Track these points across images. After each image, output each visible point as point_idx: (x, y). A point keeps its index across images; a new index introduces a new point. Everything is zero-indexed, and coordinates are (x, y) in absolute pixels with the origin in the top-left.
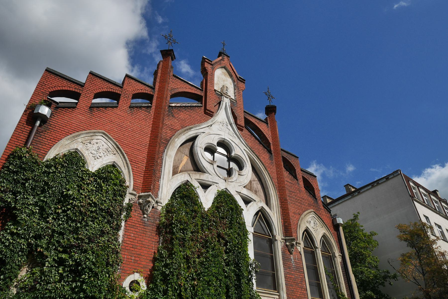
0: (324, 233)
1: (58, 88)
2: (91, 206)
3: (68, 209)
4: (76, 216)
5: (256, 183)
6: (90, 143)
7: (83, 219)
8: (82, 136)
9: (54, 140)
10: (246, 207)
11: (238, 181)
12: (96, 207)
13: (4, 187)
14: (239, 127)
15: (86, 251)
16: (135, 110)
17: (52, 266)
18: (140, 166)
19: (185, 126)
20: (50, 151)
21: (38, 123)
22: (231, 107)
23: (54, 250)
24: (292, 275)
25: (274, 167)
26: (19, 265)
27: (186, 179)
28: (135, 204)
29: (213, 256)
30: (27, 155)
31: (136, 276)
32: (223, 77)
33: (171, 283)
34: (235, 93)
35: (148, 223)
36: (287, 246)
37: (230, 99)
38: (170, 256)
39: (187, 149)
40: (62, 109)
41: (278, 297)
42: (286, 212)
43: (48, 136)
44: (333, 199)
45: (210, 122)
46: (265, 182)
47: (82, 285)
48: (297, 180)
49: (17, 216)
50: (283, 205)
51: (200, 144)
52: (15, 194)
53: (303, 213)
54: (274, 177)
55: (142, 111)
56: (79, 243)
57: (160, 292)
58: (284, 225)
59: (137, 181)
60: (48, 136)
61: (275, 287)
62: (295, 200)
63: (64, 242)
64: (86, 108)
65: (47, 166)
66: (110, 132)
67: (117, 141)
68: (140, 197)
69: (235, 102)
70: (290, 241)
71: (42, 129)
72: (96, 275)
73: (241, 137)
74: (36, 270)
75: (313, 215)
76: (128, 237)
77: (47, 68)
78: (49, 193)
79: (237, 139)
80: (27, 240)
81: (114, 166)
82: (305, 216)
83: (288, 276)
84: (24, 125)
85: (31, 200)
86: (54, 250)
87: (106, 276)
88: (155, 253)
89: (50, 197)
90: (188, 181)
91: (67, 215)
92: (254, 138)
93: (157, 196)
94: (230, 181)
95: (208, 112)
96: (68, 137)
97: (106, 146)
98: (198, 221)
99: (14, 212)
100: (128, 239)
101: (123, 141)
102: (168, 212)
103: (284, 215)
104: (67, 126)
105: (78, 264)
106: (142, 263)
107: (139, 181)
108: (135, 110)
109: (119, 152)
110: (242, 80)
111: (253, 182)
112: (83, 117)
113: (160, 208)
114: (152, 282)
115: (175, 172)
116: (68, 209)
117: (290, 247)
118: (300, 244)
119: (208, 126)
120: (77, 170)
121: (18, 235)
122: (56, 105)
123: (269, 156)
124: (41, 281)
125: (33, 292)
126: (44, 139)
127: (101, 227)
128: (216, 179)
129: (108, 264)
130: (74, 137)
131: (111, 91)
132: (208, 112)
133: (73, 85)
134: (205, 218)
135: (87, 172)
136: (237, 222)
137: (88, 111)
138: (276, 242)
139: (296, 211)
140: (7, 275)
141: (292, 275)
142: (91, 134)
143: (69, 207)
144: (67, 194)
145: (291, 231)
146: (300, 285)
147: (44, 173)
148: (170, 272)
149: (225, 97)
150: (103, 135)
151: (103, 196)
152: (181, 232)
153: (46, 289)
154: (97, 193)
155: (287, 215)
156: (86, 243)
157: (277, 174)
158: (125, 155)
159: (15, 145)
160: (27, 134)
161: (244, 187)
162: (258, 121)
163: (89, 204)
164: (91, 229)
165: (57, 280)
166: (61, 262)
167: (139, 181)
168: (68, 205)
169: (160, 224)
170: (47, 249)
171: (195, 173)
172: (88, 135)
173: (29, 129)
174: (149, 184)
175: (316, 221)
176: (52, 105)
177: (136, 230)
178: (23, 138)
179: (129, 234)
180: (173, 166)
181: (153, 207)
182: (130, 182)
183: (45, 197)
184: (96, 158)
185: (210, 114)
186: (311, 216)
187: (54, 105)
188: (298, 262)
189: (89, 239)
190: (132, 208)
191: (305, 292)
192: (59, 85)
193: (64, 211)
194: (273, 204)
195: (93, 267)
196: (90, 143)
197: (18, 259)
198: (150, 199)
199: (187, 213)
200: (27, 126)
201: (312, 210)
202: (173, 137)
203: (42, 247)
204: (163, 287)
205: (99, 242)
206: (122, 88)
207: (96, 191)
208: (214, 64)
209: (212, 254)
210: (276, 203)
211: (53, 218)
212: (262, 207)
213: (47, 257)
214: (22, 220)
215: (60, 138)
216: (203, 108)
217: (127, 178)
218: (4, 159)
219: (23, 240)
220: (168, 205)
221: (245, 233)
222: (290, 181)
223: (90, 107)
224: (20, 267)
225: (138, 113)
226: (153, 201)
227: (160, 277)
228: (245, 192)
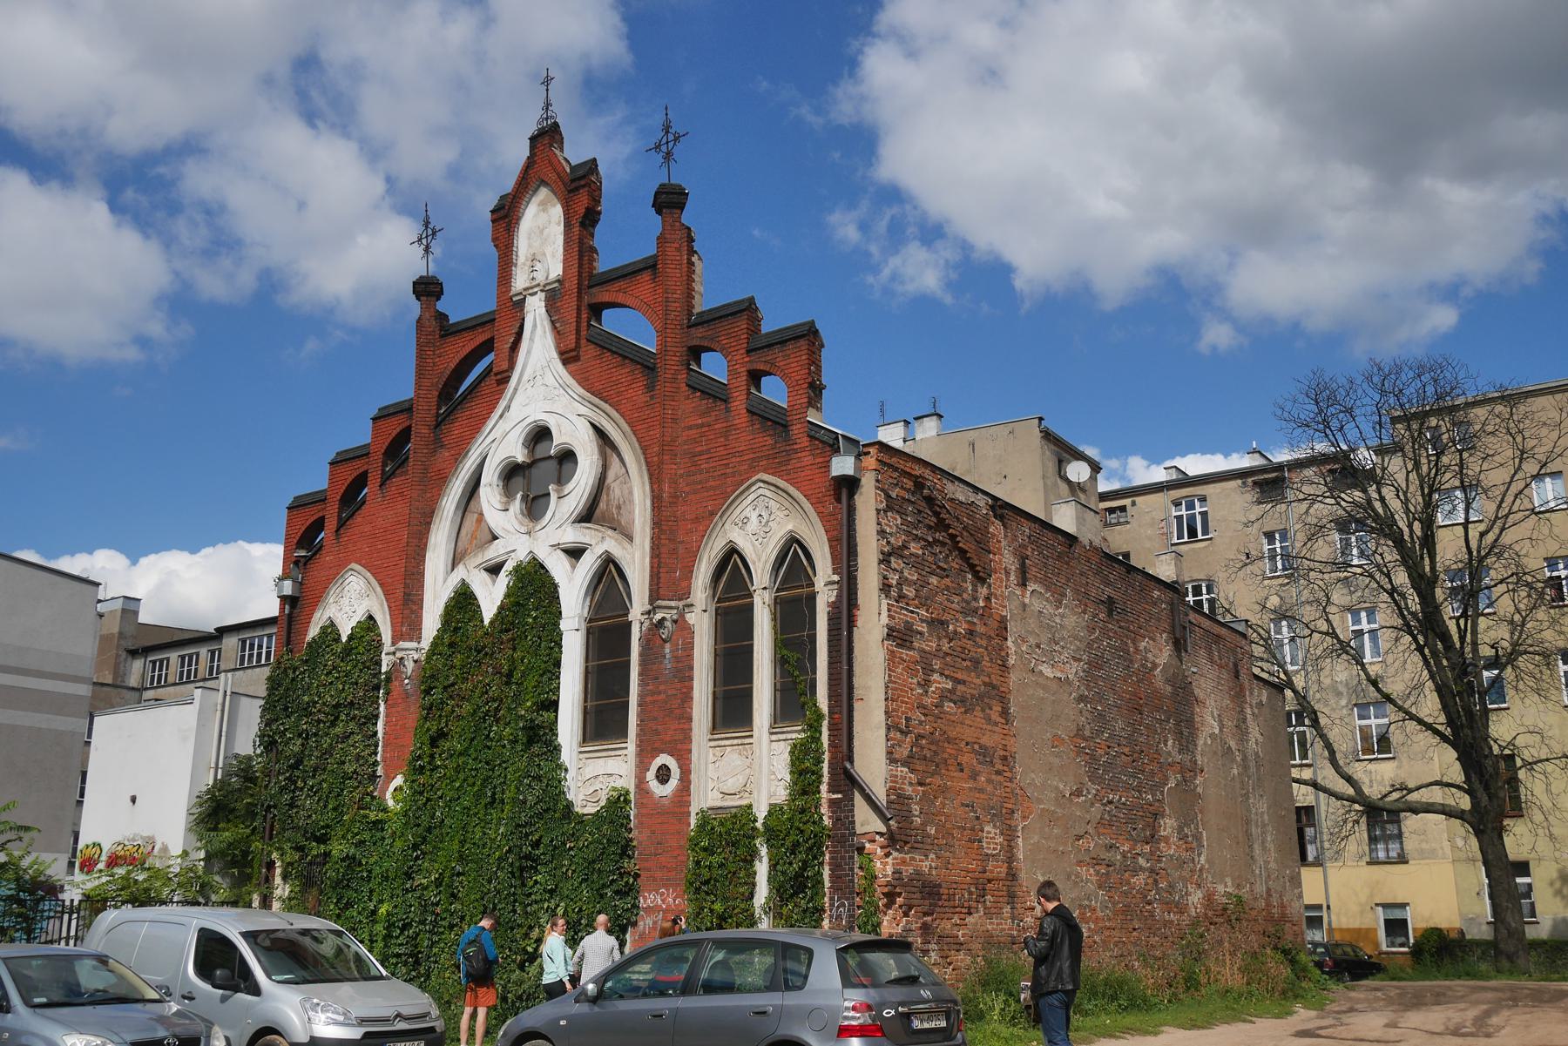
0: (791, 531)
5: (621, 483)
10: (573, 567)
32: (543, 217)
37: (542, 291)
48: (725, 401)
51: (490, 476)
69: (556, 285)
75: (761, 491)
92: (609, 354)
111: (612, 485)
118: (692, 605)
119: (501, 416)
141: (660, 693)
149: (531, 295)
162: (622, 284)
181: (416, 662)
188: (685, 654)
223: (336, 531)
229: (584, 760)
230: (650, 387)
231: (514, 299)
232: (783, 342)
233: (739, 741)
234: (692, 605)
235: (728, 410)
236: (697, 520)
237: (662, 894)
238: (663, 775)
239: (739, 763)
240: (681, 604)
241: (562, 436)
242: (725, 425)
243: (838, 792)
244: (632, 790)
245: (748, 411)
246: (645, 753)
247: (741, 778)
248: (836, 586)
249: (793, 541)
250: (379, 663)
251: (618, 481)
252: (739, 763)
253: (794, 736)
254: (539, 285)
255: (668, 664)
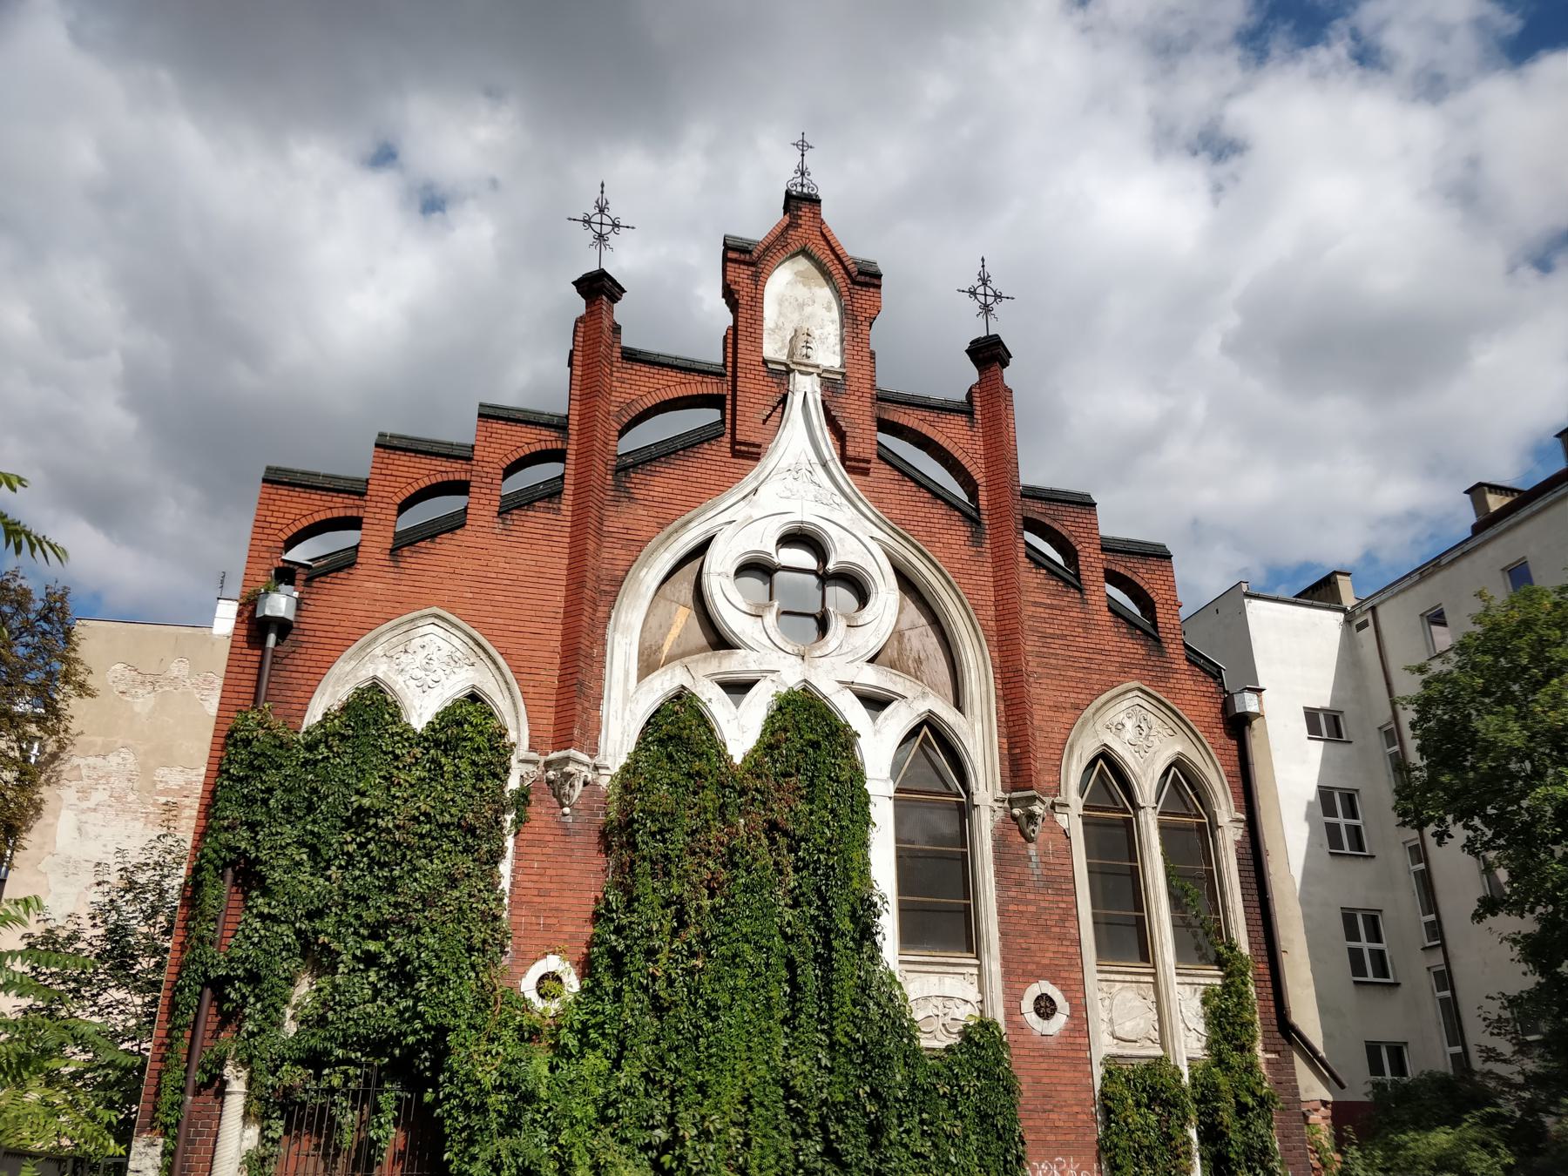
0: (1180, 753)
1: (303, 520)
2: (419, 823)
3: (369, 841)
4: (387, 853)
5: (921, 634)
6: (406, 652)
7: (404, 856)
8: (384, 639)
9: (317, 670)
11: (845, 649)
12: (429, 822)
13: (227, 818)
14: (853, 464)
15: (418, 930)
16: (515, 517)
17: (353, 970)
18: (543, 678)
19: (667, 519)
20: (313, 700)
21: (272, 638)
22: (823, 402)
23: (354, 933)
24: (1028, 902)
25: (988, 568)
26: (286, 979)
27: (676, 683)
28: (537, 784)
29: (747, 889)
30: (261, 732)
31: (552, 963)
32: (801, 292)
33: (629, 972)
34: (842, 340)
35: (577, 826)
36: (1014, 818)
37: (819, 375)
38: (631, 902)
39: (686, 585)
40: (323, 579)
41: (975, 971)
42: (1018, 712)
43: (301, 663)
44: (1519, 492)
45: (748, 483)
46: (949, 625)
47: (415, 1005)
48: (1080, 590)
49: (264, 878)
50: (1007, 692)
52: (252, 826)
53: (1092, 701)
54: (983, 603)
55: (538, 514)
56: (401, 914)
57: (608, 994)
58: (1010, 754)
59: (539, 721)
60: (301, 663)
61: (969, 941)
62: (1064, 663)
63: (369, 916)
64: (382, 557)
65: (310, 747)
66: (453, 605)
67: (475, 625)
68: (548, 765)
69: (839, 377)
70: (1023, 803)
71: (287, 646)
72: (443, 980)
73: (860, 499)
74: (324, 981)
76: (526, 871)
77: (269, 469)
78: (321, 812)
79: (845, 509)
80: (293, 924)
81: (474, 697)
82: (1098, 710)
83: (1012, 907)
84: (244, 651)
85: (289, 833)
86: (354, 933)
87: (469, 979)
88: (597, 899)
89: (326, 820)
90: (683, 687)
91: (368, 854)
93: (593, 751)
94: (818, 653)
95: (743, 448)
96: (350, 651)
97: (446, 648)
98: (709, 797)
99: (258, 868)
100: (526, 878)
101: (490, 620)
102: (626, 788)
103: (1011, 724)
104: (342, 624)
105: (404, 960)
106: (566, 929)
107: (545, 722)
108: (515, 517)
109: (483, 656)
110: (867, 279)
111: (907, 633)
112: (379, 586)
113: (604, 781)
114: (590, 976)
115: (649, 664)
116: (369, 841)
117: (1024, 819)
118: (1067, 806)
120: (379, 736)
121: (274, 919)
122: (306, 571)
123: (968, 534)
124: (335, 1004)
125: (323, 1027)
126: (294, 675)
127: (448, 867)
128: (774, 660)
129: (470, 949)
130: (362, 648)
131: (440, 480)
132: (743, 448)
133: (338, 500)
134: (728, 786)
135: (407, 736)
136: (830, 778)
137: (387, 563)
138: (975, 813)
139: (1061, 699)
140: (267, 1002)
141: (1028, 902)
142: (406, 628)
143: (369, 834)
144: (360, 805)
145: (1028, 772)
146: (1057, 930)
147: (304, 764)
148: (627, 947)
149: (801, 373)
150: (436, 621)
151: (446, 789)
152: (657, 841)
153: (348, 1019)
154: (433, 784)
155: (1020, 722)
156: (416, 911)
157: (997, 587)
158: (500, 660)
159: (234, 708)
160: (250, 684)
161: (872, 661)
163: (415, 819)
164: (425, 876)
165: (367, 997)
166: (371, 960)
167: (545, 722)
168: (368, 829)
169: (606, 825)
170: (337, 936)
171: (705, 659)
172: (396, 632)
173: (255, 659)
174: (569, 725)
175: (1150, 717)
176: (298, 577)
177: (545, 851)
178: (247, 684)
179: (527, 864)
180: (641, 654)
181: (586, 784)
182: (519, 733)
183: (314, 822)
184: (425, 688)
185: (749, 453)
186: (1126, 704)
187: (301, 576)
189: (423, 898)
190: (531, 797)
191: (1072, 950)
192: (304, 512)
193: (361, 846)
194: (971, 693)
195: (435, 963)
196: (406, 652)
197: (283, 967)
198: (571, 768)
199: (673, 784)
200: (250, 652)
201: (1136, 684)
202: (635, 566)
203: (327, 934)
204: (608, 983)
205: (445, 904)
206: (471, 459)
207: (432, 779)
208: (759, 258)
209: (744, 885)
210: (984, 688)
211: (340, 867)
212: (930, 711)
213: (339, 954)
214: (276, 884)
215: (331, 659)
216: (727, 439)
217: (509, 722)
218: (218, 747)
219: (284, 927)
220: (625, 769)
221: (860, 803)
222: (1049, 601)
223: (392, 550)
224: (291, 981)
225: (526, 524)
226: (584, 768)
227: (606, 961)
228: (872, 678)
229: (904, 974)
230: (976, 539)
231: (770, 366)
232: (1145, 555)
233: (1134, 978)
234: (1067, 806)
235: (1084, 602)
236: (1056, 708)
237: (1059, 1164)
238: (1045, 1007)
239: (1138, 1004)
240: (1048, 800)
241: (843, 553)
242: (1082, 615)
243: (1272, 1052)
244: (1000, 1018)
245: (1110, 609)
246: (1016, 975)
247: (1142, 1022)
248: (1242, 825)
249: (1178, 763)
250: (507, 771)
251: (917, 631)
252: (1138, 1004)
253: (1208, 981)
254: (817, 367)
255: (1035, 869)
